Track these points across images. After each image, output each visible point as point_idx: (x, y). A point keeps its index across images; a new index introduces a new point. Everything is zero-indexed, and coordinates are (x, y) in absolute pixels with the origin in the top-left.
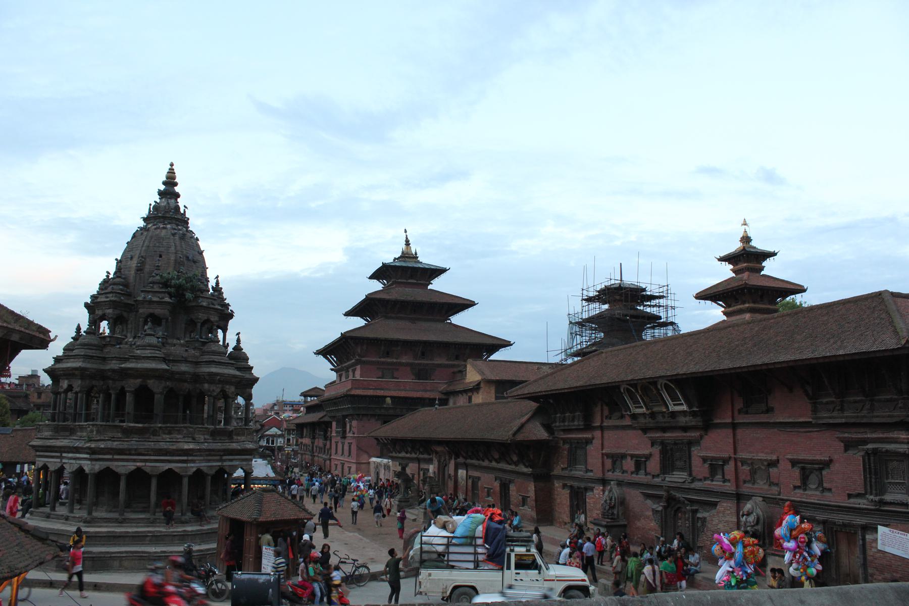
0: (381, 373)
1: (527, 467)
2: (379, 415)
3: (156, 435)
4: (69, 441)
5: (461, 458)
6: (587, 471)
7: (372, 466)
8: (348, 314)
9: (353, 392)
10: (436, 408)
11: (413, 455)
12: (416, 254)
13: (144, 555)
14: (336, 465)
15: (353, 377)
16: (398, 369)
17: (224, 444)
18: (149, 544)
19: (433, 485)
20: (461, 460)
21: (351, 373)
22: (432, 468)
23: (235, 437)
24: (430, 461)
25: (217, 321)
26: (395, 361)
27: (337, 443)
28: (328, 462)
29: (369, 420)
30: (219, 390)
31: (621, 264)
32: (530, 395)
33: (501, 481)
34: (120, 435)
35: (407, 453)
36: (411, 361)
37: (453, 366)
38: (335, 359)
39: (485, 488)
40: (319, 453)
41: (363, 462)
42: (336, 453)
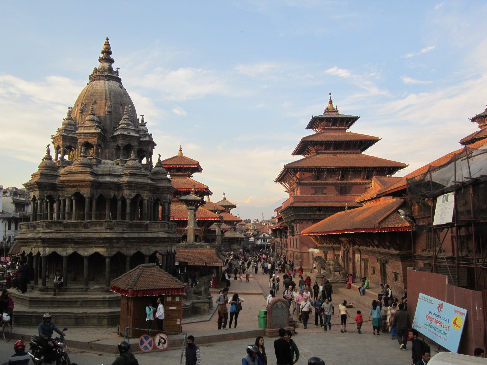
0: (314, 191)
1: (396, 249)
2: (314, 220)
3: (86, 228)
4: (32, 234)
5: (356, 245)
6: (440, 251)
8: (294, 154)
11: (331, 245)
12: (337, 108)
13: (71, 315)
15: (297, 194)
16: (325, 188)
17: (140, 234)
18: (80, 307)
20: (356, 247)
21: (295, 192)
22: (341, 253)
23: (150, 229)
24: (339, 249)
25: (136, 146)
26: (323, 182)
29: (307, 223)
30: (134, 195)
32: (391, 192)
33: (381, 261)
34: (62, 228)
35: (327, 244)
36: (334, 181)
38: (288, 185)
39: (372, 267)
40: (284, 247)
42: (290, 247)
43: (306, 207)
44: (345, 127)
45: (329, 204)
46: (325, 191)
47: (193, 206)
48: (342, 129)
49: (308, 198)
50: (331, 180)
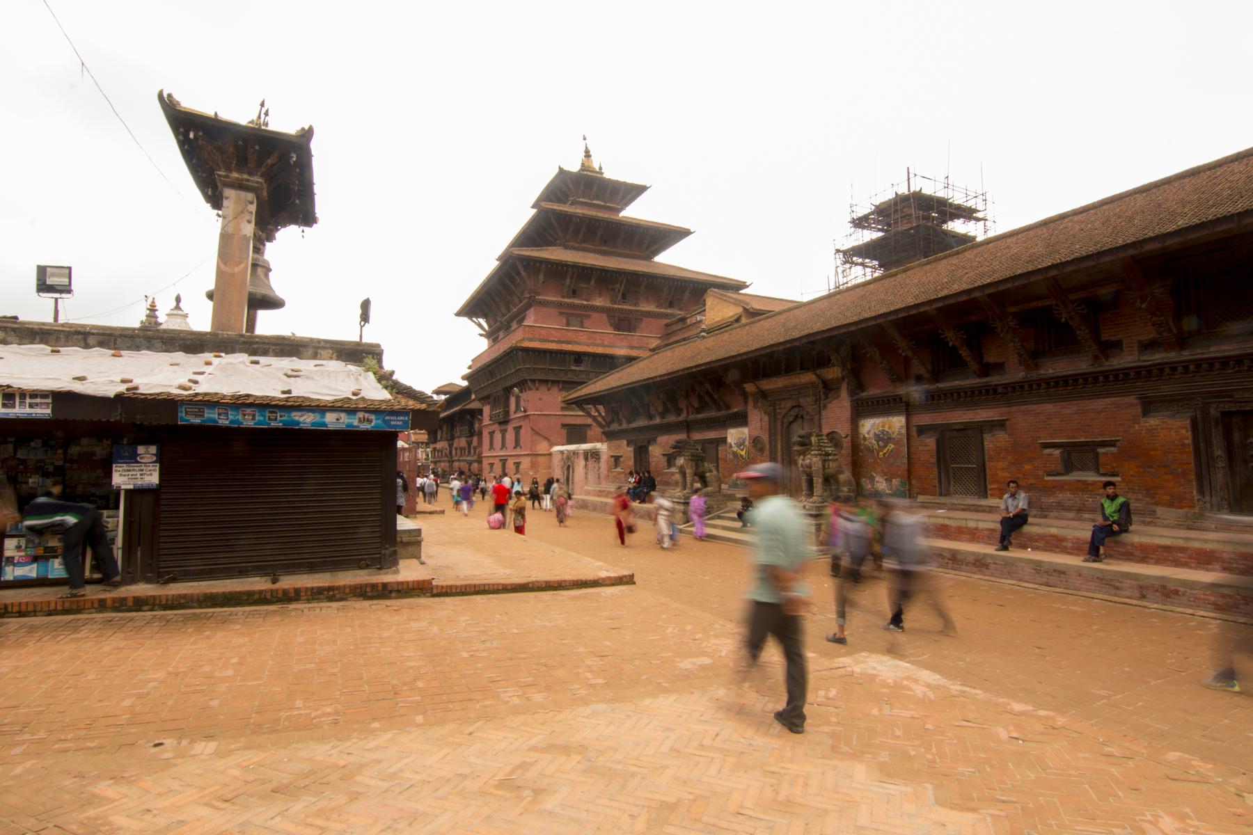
0: (565, 321)
2: (564, 382)
7: (556, 461)
9: (526, 344)
10: (704, 337)
11: (671, 418)
12: (600, 168)
14: (492, 465)
16: (588, 317)
19: (829, 455)
26: (585, 303)
27: (492, 434)
28: (475, 465)
29: (549, 390)
31: (908, 168)
35: (651, 417)
36: (608, 305)
37: (666, 316)
40: (460, 457)
41: (541, 453)
43: (551, 352)
44: (618, 205)
45: (600, 350)
46: (586, 323)
47: (250, 174)
48: (613, 207)
49: (553, 332)
50: (600, 302)
